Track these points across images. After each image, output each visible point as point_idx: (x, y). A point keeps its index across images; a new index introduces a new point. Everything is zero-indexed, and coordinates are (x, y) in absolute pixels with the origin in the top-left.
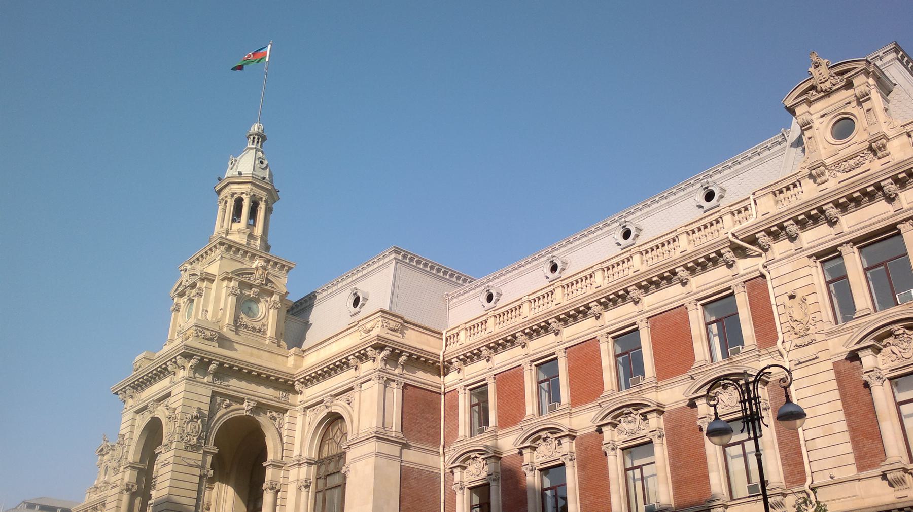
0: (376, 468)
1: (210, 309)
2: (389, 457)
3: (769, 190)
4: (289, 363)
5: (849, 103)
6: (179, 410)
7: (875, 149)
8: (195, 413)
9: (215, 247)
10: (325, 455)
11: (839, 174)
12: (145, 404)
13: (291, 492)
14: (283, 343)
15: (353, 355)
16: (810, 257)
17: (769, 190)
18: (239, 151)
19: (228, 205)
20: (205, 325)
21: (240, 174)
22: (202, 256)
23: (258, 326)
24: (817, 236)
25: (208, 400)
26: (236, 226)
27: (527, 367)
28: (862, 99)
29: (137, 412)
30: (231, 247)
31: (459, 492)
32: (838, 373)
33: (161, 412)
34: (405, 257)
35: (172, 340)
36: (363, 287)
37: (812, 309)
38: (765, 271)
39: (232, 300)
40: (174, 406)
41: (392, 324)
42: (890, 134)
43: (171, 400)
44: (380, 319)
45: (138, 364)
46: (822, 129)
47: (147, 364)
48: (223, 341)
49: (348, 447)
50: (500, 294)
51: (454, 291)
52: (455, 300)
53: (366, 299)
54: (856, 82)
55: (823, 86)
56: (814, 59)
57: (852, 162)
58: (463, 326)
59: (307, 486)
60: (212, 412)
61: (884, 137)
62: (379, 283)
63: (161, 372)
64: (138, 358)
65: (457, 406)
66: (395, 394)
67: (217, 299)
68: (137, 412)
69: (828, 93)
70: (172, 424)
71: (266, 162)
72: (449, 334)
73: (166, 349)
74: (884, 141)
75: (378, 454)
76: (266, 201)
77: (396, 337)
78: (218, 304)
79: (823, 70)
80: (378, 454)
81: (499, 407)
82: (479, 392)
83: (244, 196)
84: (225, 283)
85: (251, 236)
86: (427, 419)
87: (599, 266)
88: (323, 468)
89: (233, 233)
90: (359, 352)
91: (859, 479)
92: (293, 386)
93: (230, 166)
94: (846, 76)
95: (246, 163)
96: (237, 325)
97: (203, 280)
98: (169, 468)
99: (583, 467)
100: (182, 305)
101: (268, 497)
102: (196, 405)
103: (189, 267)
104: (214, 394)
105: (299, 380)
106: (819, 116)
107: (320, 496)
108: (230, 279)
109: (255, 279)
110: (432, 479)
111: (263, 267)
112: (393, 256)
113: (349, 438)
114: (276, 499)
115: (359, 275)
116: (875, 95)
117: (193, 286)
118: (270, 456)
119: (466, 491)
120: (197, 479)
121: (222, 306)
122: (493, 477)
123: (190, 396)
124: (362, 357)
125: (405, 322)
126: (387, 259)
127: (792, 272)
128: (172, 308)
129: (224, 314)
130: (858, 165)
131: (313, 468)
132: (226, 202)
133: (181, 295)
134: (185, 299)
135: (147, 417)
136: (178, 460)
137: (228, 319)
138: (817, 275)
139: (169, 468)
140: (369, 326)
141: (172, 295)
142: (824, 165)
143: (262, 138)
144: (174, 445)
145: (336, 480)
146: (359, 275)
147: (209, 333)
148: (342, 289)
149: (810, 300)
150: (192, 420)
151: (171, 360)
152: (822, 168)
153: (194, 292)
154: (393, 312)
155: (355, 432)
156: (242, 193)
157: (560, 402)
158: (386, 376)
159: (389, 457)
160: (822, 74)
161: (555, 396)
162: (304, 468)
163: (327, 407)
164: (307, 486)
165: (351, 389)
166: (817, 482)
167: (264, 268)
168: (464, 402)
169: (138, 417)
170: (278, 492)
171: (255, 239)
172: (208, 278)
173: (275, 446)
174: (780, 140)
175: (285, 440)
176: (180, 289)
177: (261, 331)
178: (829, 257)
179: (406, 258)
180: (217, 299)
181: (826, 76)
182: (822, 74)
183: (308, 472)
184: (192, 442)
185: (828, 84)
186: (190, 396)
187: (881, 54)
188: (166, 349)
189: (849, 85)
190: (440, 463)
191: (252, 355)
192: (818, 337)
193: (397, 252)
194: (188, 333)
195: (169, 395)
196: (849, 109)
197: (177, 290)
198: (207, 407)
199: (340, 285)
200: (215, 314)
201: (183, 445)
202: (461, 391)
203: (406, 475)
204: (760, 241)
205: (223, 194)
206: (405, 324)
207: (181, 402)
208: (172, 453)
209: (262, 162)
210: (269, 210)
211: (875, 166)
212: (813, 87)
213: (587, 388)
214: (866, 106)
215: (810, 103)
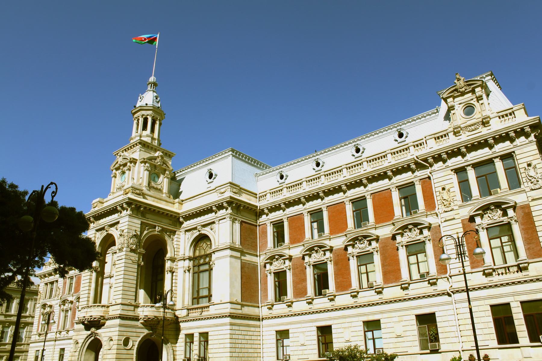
0: (231, 263)
1: (135, 178)
2: (236, 257)
3: (433, 136)
4: (175, 208)
5: (472, 99)
6: (126, 231)
7: (485, 123)
8: (134, 233)
9: (136, 144)
10: (197, 254)
11: (467, 132)
12: (103, 226)
13: (180, 273)
14: (172, 197)
15: (215, 205)
16: (452, 170)
17: (433, 136)
18: (144, 91)
19: (140, 121)
20: (136, 187)
21: (147, 104)
22: (128, 149)
23: (159, 187)
24: (457, 161)
25: (139, 226)
26: (145, 133)
27: (306, 214)
28: (479, 98)
29: (97, 231)
30: (144, 145)
31: (269, 275)
32: (463, 225)
33: (113, 231)
34: (236, 153)
35: (113, 193)
36: (215, 168)
37: (452, 194)
38: (430, 175)
39: (147, 173)
40: (122, 228)
41: (235, 190)
42: (491, 116)
43: (119, 225)
44: (229, 187)
45: (95, 205)
46: (459, 111)
48: (144, 195)
49: (214, 252)
50: (287, 176)
51: (259, 171)
52: (260, 177)
53: (216, 175)
54: (477, 90)
55: (461, 90)
56: (458, 76)
57: (473, 127)
58: (269, 191)
59: (189, 271)
60: (142, 232)
61: (489, 117)
62: (225, 167)
63: (113, 211)
64: (94, 201)
65: (266, 232)
66: (237, 226)
67: (139, 173)
68: (97, 231)
69: (463, 94)
70: (122, 239)
71: (159, 99)
72: (260, 195)
74: (489, 119)
75: (231, 256)
76: (159, 120)
77: (236, 197)
78: (139, 175)
79: (462, 82)
80: (231, 256)
81: (290, 234)
82: (278, 226)
83: (148, 117)
84: (143, 164)
85: (153, 139)
86: (251, 238)
87: (345, 166)
88: (197, 261)
89: (144, 137)
90: (218, 204)
91: (472, 273)
92: (179, 219)
93: (140, 100)
94: (472, 86)
95: (148, 98)
96: (150, 187)
97: (131, 162)
98: (123, 261)
99: (336, 264)
100: (118, 175)
101: (168, 277)
102: (135, 229)
103: (122, 154)
104: (142, 223)
105: (182, 216)
106: (459, 103)
107: (196, 275)
108: (145, 163)
109: (157, 163)
110: (254, 267)
111: (161, 156)
112: (231, 153)
113: (213, 247)
114: (172, 276)
115: (210, 161)
116: (484, 96)
117: (125, 165)
118: (168, 255)
119: (272, 274)
120: (136, 267)
121: (141, 176)
122: (288, 268)
123: (131, 224)
124: (220, 207)
125: (241, 188)
126: (226, 154)
127: (443, 176)
128: (112, 176)
129: (143, 181)
130: (476, 129)
131: (192, 261)
132: (138, 120)
133: (117, 169)
134: (120, 171)
135: (104, 233)
137: (145, 183)
138: (454, 179)
139: (123, 261)
140: (222, 190)
141: (112, 168)
142: (460, 127)
143: (155, 84)
144: (125, 249)
145: (206, 267)
146: (210, 161)
147: (138, 191)
148: (200, 168)
149: (451, 190)
150: (133, 237)
151: (119, 205)
152: (459, 129)
153: (125, 168)
154: (234, 182)
155: (217, 244)
156: (148, 115)
157: (324, 232)
158: (233, 217)
159: (236, 257)
160: (461, 84)
161: (321, 229)
162: (187, 261)
163: (199, 231)
164: (189, 271)
165: (214, 223)
166: (452, 274)
167: (162, 157)
168: (270, 230)
169: (98, 234)
170: (174, 272)
171: (155, 139)
172: (134, 161)
173: (171, 249)
174: (435, 111)
175: (175, 246)
176: (117, 166)
177: (160, 190)
178: (460, 171)
179: (237, 155)
180: (139, 173)
181: (463, 85)
182: (461, 84)
183: (189, 264)
184: (133, 248)
185: (463, 89)
186: (131, 224)
187: (484, 76)
189: (473, 91)
190: (260, 261)
191: (157, 202)
192: (455, 208)
193: (233, 151)
194: (127, 190)
195: (118, 223)
196: (472, 102)
197: (115, 166)
198: (139, 230)
199: (198, 166)
200: (138, 180)
201: (129, 250)
202: (268, 225)
203: (244, 266)
204: (429, 161)
205: (136, 115)
206: (241, 190)
207: (127, 227)
208: (124, 253)
209: (157, 99)
210: (160, 124)
211: (484, 131)
212: (456, 90)
213: (339, 226)
214: (481, 102)
215: (454, 98)
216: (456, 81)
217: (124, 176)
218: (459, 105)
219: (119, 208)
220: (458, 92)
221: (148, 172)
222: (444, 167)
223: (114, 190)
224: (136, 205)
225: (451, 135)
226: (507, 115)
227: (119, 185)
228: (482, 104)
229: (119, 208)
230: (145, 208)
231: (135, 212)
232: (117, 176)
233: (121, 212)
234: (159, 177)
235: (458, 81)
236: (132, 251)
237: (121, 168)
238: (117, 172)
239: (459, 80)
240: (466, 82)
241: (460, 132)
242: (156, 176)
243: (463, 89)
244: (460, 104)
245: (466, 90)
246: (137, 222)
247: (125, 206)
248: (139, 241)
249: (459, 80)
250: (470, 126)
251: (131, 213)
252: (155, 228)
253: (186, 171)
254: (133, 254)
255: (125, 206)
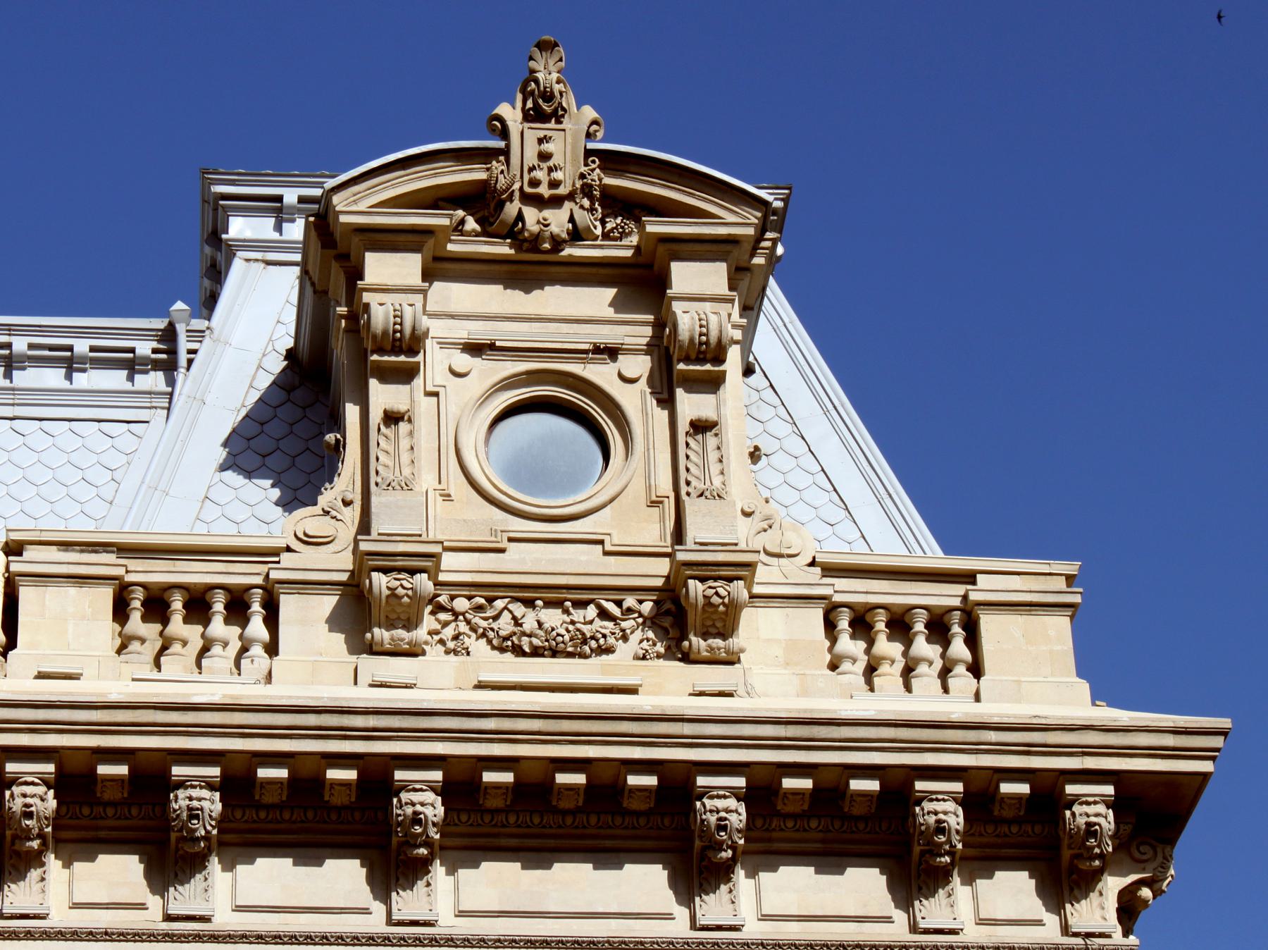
3: (107, 564)
5: (612, 352)
7: (686, 616)
11: (479, 647)
17: (107, 564)
54: (688, 277)
56: (548, 72)
69: (533, 265)
79: (566, 147)
94: (656, 227)
174: (145, 348)
181: (567, 178)
185: (558, 221)
196: (601, 374)
214: (690, 405)
216: (511, 113)
218: (463, 361)
220: (489, 229)
222: (151, 918)
225: (307, 618)
226: (900, 625)
228: (701, 427)
235: (534, 116)
239: (543, 111)
240: (612, 162)
241: (411, 623)
243: (558, 221)
244: (475, 349)
245: (577, 235)
249: (543, 111)
250: (528, 595)
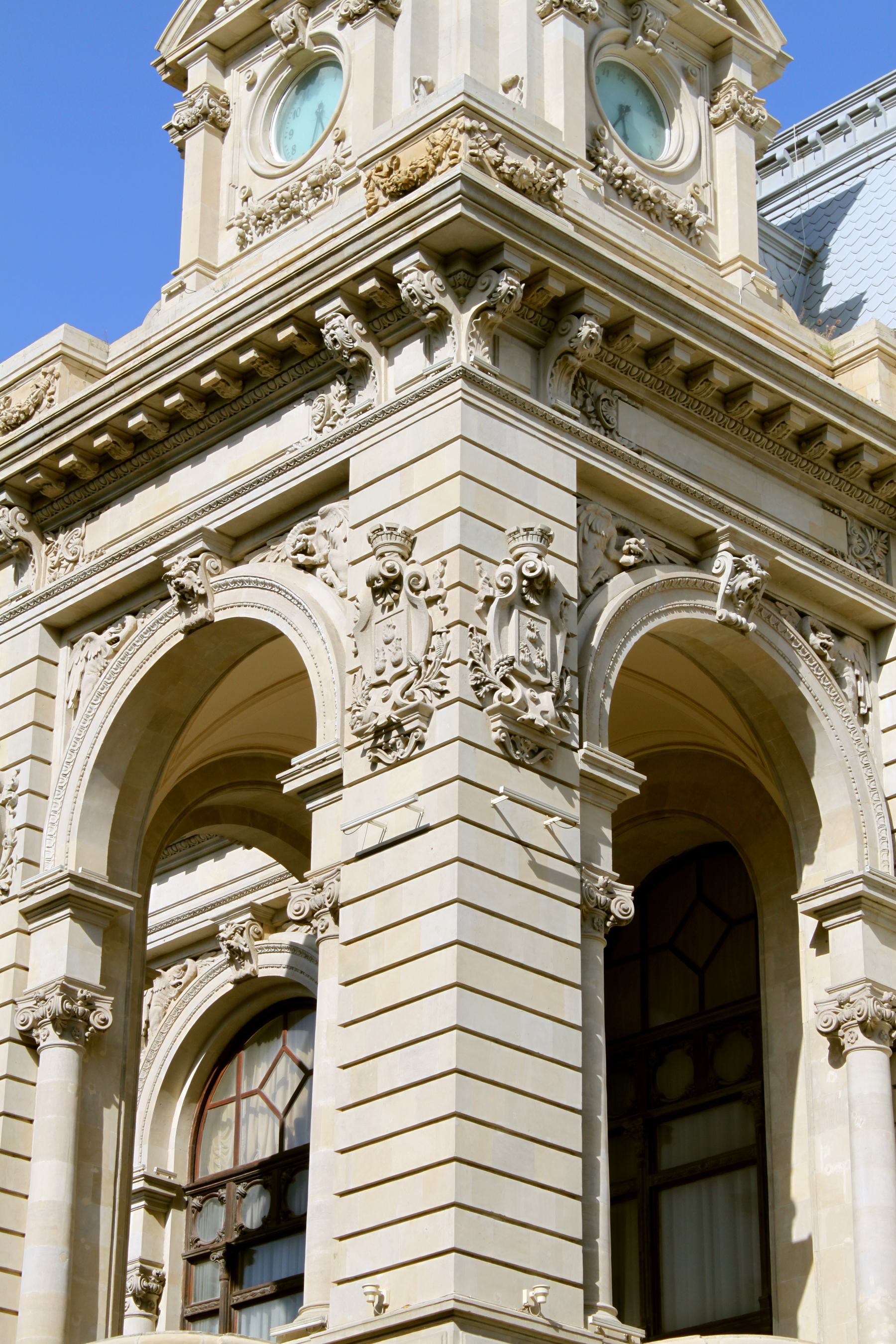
23: (680, 199)
47: (69, 390)
63: (284, 364)
68: (62, 631)
73: (169, 316)
133: (229, 52)
134: (263, 64)
136: (481, 807)
141: (171, 48)
144: (445, 724)
188: (169, 316)
201: (492, 730)
217: (306, 108)
219: (342, 328)
221: (578, 35)
223: (208, 238)
224: (534, 281)
227: (262, 188)
229: (342, 328)
230: (615, 330)
231: (518, 362)
232: (237, 119)
233: (356, 374)
234: (660, 115)
236: (528, 746)
237: (280, 22)
238: (234, 84)
242: (638, 106)
246: (543, 466)
247: (418, 280)
248: (581, 662)
251: (482, 353)
252: (700, 550)
253: (863, 132)
254: (528, 783)
255: (418, 280)
